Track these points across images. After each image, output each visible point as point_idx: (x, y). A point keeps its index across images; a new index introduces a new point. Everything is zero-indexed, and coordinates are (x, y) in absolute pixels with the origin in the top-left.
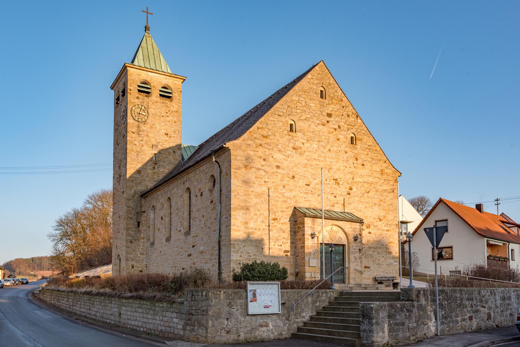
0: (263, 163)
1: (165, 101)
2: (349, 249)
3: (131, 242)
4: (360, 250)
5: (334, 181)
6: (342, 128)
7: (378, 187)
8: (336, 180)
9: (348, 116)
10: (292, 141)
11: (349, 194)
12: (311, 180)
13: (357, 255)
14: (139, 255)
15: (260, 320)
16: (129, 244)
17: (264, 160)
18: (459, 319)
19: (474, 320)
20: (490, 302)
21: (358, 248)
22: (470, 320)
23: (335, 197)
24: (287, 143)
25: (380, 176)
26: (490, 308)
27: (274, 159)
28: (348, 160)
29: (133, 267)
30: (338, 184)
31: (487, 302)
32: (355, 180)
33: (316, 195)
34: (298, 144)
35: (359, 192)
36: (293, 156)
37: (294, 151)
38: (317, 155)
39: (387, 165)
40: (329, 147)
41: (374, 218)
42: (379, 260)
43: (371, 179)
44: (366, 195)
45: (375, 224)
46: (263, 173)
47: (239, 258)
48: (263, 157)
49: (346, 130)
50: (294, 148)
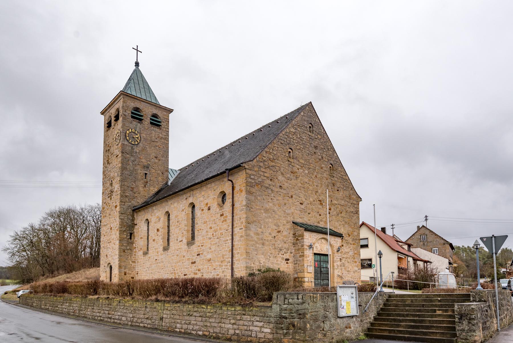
0: (270, 183)
1: (155, 129)
3: (124, 251)
5: (319, 202)
7: (348, 209)
12: (304, 200)
14: (131, 263)
16: (122, 254)
23: (320, 215)
24: (287, 168)
27: (278, 180)
29: (125, 274)
32: (333, 202)
33: (307, 213)
34: (295, 169)
35: (335, 213)
43: (343, 202)
45: (346, 239)
46: (270, 192)
47: (252, 265)
50: (292, 172)
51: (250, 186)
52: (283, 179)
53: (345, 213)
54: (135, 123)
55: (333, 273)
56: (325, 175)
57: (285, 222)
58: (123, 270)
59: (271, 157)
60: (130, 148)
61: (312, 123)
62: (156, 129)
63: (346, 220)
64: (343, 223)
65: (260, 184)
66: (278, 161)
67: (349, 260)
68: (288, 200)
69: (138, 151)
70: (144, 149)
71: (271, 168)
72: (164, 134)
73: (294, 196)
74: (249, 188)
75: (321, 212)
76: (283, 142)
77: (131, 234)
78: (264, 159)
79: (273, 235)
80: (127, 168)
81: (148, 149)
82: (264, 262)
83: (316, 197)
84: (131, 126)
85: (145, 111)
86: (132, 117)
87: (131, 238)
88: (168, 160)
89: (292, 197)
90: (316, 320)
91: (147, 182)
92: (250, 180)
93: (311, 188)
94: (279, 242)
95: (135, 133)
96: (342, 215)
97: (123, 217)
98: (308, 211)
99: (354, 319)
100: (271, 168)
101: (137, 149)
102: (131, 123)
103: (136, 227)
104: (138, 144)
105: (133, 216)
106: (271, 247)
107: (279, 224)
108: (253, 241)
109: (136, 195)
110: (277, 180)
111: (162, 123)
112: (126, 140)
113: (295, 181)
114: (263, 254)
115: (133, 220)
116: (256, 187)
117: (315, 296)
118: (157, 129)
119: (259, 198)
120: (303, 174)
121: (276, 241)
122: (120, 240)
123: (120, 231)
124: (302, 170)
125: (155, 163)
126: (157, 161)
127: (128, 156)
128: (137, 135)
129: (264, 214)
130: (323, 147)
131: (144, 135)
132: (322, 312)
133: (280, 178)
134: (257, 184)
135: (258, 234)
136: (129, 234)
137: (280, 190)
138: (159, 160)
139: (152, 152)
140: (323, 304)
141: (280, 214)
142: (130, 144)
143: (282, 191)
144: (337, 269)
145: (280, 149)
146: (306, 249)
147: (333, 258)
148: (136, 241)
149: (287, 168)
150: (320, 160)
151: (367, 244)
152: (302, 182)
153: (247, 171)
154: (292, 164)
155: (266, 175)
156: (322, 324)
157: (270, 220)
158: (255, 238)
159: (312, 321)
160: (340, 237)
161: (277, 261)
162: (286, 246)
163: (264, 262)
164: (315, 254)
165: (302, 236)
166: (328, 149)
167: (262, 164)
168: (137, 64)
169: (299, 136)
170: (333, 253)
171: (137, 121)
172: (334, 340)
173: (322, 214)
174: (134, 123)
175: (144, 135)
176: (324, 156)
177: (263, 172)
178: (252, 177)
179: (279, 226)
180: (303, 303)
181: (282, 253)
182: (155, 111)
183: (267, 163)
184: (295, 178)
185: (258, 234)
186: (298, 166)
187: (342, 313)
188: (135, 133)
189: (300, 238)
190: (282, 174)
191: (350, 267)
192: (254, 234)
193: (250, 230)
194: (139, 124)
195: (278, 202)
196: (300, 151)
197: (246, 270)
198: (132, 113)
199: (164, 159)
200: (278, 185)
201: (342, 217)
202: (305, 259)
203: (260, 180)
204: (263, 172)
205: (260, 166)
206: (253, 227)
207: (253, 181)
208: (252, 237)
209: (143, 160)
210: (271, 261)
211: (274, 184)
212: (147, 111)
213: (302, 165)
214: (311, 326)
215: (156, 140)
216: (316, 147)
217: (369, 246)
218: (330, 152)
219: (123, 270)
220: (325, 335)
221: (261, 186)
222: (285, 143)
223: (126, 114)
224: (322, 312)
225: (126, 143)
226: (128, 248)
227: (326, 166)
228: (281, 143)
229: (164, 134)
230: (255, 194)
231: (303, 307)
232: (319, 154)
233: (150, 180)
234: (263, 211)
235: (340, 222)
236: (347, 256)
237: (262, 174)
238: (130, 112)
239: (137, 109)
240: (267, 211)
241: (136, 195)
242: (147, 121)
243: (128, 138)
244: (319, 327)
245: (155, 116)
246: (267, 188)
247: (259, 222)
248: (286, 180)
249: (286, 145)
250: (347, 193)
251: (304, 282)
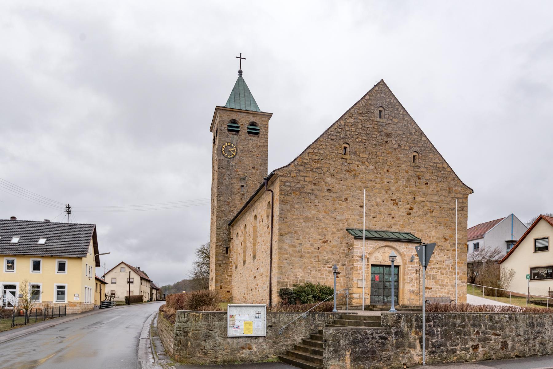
0: (314, 187)
1: (252, 138)
5: (392, 202)
7: (444, 205)
8: (395, 200)
10: (346, 164)
11: (410, 214)
15: (242, 342)
17: (315, 184)
18: (458, 348)
19: (480, 349)
20: (507, 330)
22: (473, 349)
23: (393, 218)
24: (340, 167)
25: (447, 194)
26: (506, 337)
27: (326, 183)
28: (408, 180)
30: (397, 204)
31: (502, 329)
32: (417, 200)
33: (371, 217)
34: (353, 167)
35: (421, 212)
36: (347, 180)
37: (347, 174)
38: (373, 176)
39: (456, 182)
40: (387, 167)
43: (436, 198)
44: (429, 215)
45: (440, 244)
46: (313, 197)
48: (314, 182)
50: (348, 171)
51: (284, 195)
52: (334, 180)
53: (439, 212)
54: (232, 136)
56: (404, 167)
57: (335, 230)
58: (219, 284)
59: (316, 157)
60: (226, 163)
62: (254, 138)
63: (442, 220)
64: (435, 224)
65: (300, 191)
66: (326, 161)
67: (445, 272)
68: (340, 205)
69: (234, 164)
70: (240, 161)
71: (315, 170)
72: (262, 141)
73: (350, 199)
74: (282, 197)
75: (395, 213)
76: (334, 137)
78: (306, 161)
79: (316, 246)
80: (222, 183)
81: (245, 160)
82: (302, 277)
83: (386, 196)
84: (227, 139)
85: (242, 122)
86: (229, 130)
88: (267, 169)
89: (346, 200)
90: (196, 338)
91: (243, 195)
92: (284, 188)
93: (378, 186)
94: (325, 253)
95: (231, 146)
96: (434, 214)
97: (219, 233)
98: (373, 215)
99: (261, 340)
100: (315, 170)
101: (233, 163)
102: (227, 136)
103: (232, 241)
104: (235, 156)
105: (229, 230)
106: (313, 260)
107: (326, 233)
108: (287, 254)
109: (232, 209)
110: (323, 183)
111: (261, 130)
112: (222, 156)
113: (353, 181)
114: (301, 268)
116: (293, 194)
117: (197, 315)
118: (254, 138)
119: (296, 206)
120: (365, 171)
122: (216, 255)
123: (216, 246)
124: (363, 167)
125: (252, 174)
126: (254, 171)
127: (224, 170)
128: (233, 148)
129: (303, 224)
131: (241, 147)
132: (204, 331)
133: (329, 180)
134: (294, 191)
135: (294, 246)
137: (329, 194)
138: (257, 170)
139: (249, 162)
140: (206, 323)
141: (326, 221)
142: (226, 159)
143: (332, 194)
145: (328, 147)
146: (358, 260)
147: (404, 269)
149: (340, 167)
150: (395, 149)
151: (546, 245)
152: (364, 181)
153: (281, 178)
154: (348, 161)
155: (307, 179)
156: (203, 343)
157: (312, 230)
158: (290, 251)
159: (192, 339)
160: (418, 243)
161: (321, 275)
163: (302, 277)
165: (352, 245)
167: (301, 168)
169: (360, 126)
171: (234, 133)
172: (219, 360)
173: (396, 216)
174: (231, 136)
175: (241, 147)
176: (403, 143)
177: (303, 176)
178: (287, 184)
179: (325, 235)
180: (187, 321)
181: (329, 266)
182: (252, 119)
183: (309, 166)
184: (351, 177)
185: (294, 246)
186: (357, 163)
187: (231, 332)
188: (231, 146)
189: (351, 248)
190: (331, 175)
191: (446, 280)
192: (289, 246)
193: (283, 242)
194: (236, 136)
195: (325, 208)
196: (361, 144)
197: (278, 285)
198: (229, 126)
199: (262, 168)
200: (326, 188)
201: (432, 217)
202: (355, 272)
203: (299, 186)
204: (303, 176)
205: (299, 170)
206: (288, 240)
207: (289, 189)
208: (285, 250)
209: (239, 173)
210: (312, 275)
211: (318, 188)
212: (244, 121)
213: (364, 160)
214: (192, 344)
215: (254, 150)
217: (550, 248)
219: (219, 284)
220: (205, 354)
221: (300, 193)
222: (338, 138)
223: (223, 128)
224: (204, 331)
225: (222, 158)
227: (406, 157)
228: (332, 139)
229: (262, 141)
230: (290, 203)
231: (186, 325)
232: (394, 142)
233: (247, 192)
234: (301, 221)
235: (428, 224)
236: (441, 266)
237: (302, 178)
238: (226, 126)
239: (234, 121)
240: (307, 219)
241: (232, 209)
242: (244, 132)
243: (224, 152)
244: (199, 345)
245: (253, 124)
246: (309, 194)
247: (296, 233)
248: (338, 182)
249: (339, 140)
250: (445, 185)
251: (353, 298)
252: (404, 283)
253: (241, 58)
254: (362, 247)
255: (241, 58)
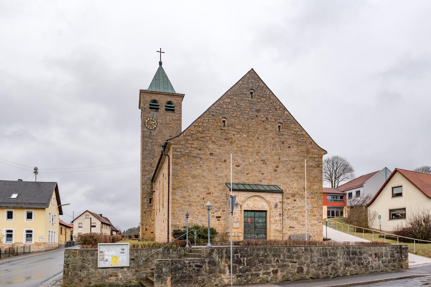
0: (199, 152)
1: (169, 114)
2: (270, 213)
3: (145, 213)
4: (280, 214)
5: (262, 162)
6: (270, 120)
8: (264, 160)
9: (276, 109)
10: (224, 134)
11: (276, 171)
12: (241, 162)
13: (278, 218)
14: (151, 221)
15: (110, 271)
16: (144, 215)
17: (200, 150)
18: (261, 272)
19: (279, 273)
20: (303, 259)
21: (278, 213)
22: (274, 273)
23: (263, 174)
24: (220, 136)
25: (305, 155)
26: (302, 263)
27: (209, 148)
28: (275, 145)
29: (146, 230)
30: (266, 164)
31: (298, 258)
32: (282, 160)
33: (245, 174)
34: (230, 136)
35: (285, 169)
36: (225, 146)
37: (226, 141)
38: (246, 143)
39: (313, 145)
40: (257, 135)
41: (299, 189)
42: (304, 221)
44: (292, 171)
45: (300, 193)
46: (198, 160)
47: (178, 223)
48: (199, 148)
49: (274, 121)
50: (226, 139)
51: (176, 158)
52: (215, 146)
53: (300, 168)
54: (152, 112)
55: (270, 227)
57: (216, 185)
59: (201, 129)
60: (149, 133)
61: (254, 89)
62: (170, 113)
64: (296, 178)
65: (188, 155)
68: (220, 165)
71: (200, 139)
72: (177, 116)
77: (151, 199)
78: (192, 132)
79: (202, 197)
84: (149, 115)
85: (160, 101)
86: (150, 108)
87: (150, 202)
89: (225, 161)
90: (74, 269)
92: (176, 153)
93: (251, 150)
95: (152, 120)
96: (295, 170)
98: (247, 172)
99: (125, 270)
100: (200, 139)
101: (154, 133)
102: (149, 113)
106: (199, 207)
107: (209, 187)
108: (179, 203)
110: (207, 149)
111: (176, 108)
112: (145, 128)
115: (152, 188)
116: (182, 158)
117: (75, 251)
119: (185, 167)
120: (239, 138)
121: (205, 202)
124: (238, 136)
127: (147, 139)
128: (154, 121)
129: (191, 180)
130: (268, 108)
131: (160, 121)
132: (80, 263)
133: (211, 146)
134: (184, 155)
135: (184, 197)
136: (149, 200)
137: (211, 157)
140: (82, 258)
141: (210, 178)
143: (214, 157)
144: (274, 224)
145: (210, 121)
148: (155, 204)
149: (220, 136)
150: (264, 122)
152: (239, 146)
154: (226, 132)
155: (193, 146)
156: (79, 272)
157: (198, 184)
158: (181, 201)
160: (281, 193)
162: (218, 205)
164: (245, 211)
166: (276, 109)
167: (189, 138)
168: (160, 63)
169: (235, 104)
170: (271, 209)
171: (154, 110)
172: (91, 285)
174: (152, 112)
175: (160, 121)
177: (190, 144)
178: (178, 150)
179: (209, 189)
180: (69, 257)
182: (169, 99)
183: (195, 136)
184: (229, 143)
185: (184, 197)
186: (233, 133)
187: (101, 264)
190: (213, 142)
194: (156, 113)
195: (208, 167)
196: (236, 118)
200: (209, 152)
201: (294, 173)
203: (187, 151)
204: (190, 144)
205: (187, 140)
206: (179, 193)
207: (179, 154)
208: (177, 200)
209: (159, 141)
211: (203, 152)
212: (162, 101)
213: (238, 131)
214: (71, 273)
215: (170, 123)
216: (258, 111)
217: (403, 194)
218: (279, 111)
220: (81, 281)
221: (188, 157)
222: (218, 114)
223: (145, 107)
224: (80, 263)
225: (146, 129)
226: (148, 210)
227: (272, 127)
229: (177, 116)
230: (180, 164)
232: (263, 116)
234: (190, 178)
235: (291, 178)
236: (302, 210)
237: (190, 146)
238: (148, 105)
239: (155, 101)
240: (194, 177)
242: (162, 109)
243: (146, 125)
244: (77, 274)
247: (185, 187)
248: (218, 147)
249: (219, 116)
250: (304, 148)
252: (270, 224)
253: (161, 52)
254: (240, 197)
255: (161, 52)
